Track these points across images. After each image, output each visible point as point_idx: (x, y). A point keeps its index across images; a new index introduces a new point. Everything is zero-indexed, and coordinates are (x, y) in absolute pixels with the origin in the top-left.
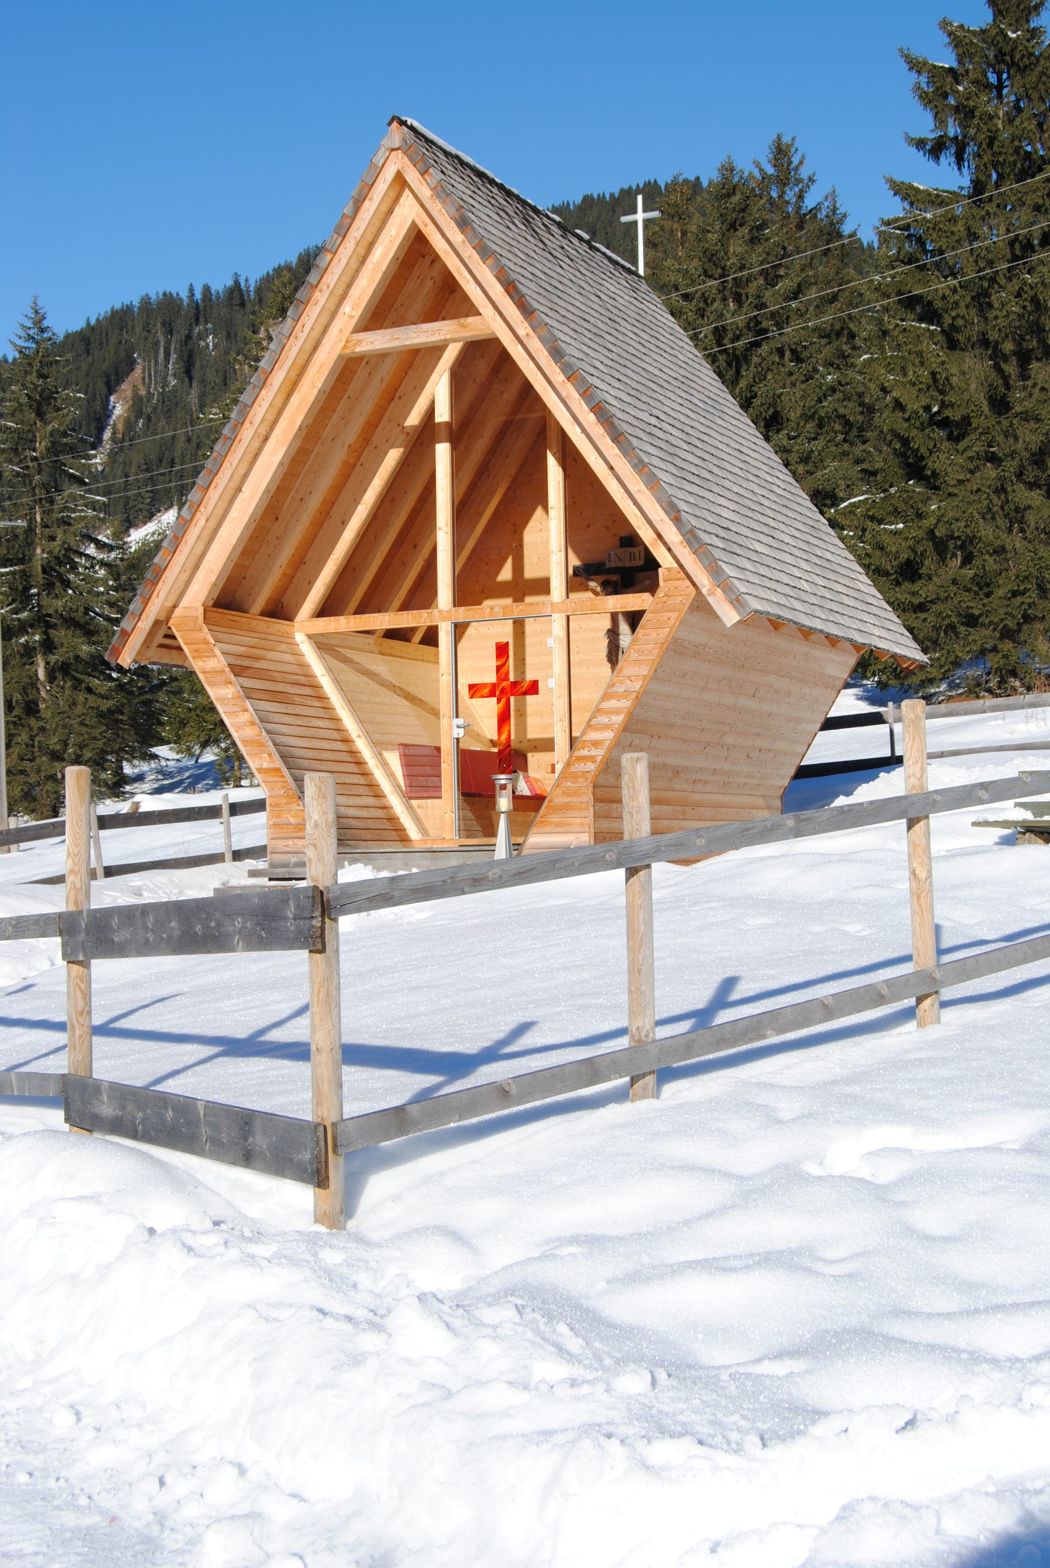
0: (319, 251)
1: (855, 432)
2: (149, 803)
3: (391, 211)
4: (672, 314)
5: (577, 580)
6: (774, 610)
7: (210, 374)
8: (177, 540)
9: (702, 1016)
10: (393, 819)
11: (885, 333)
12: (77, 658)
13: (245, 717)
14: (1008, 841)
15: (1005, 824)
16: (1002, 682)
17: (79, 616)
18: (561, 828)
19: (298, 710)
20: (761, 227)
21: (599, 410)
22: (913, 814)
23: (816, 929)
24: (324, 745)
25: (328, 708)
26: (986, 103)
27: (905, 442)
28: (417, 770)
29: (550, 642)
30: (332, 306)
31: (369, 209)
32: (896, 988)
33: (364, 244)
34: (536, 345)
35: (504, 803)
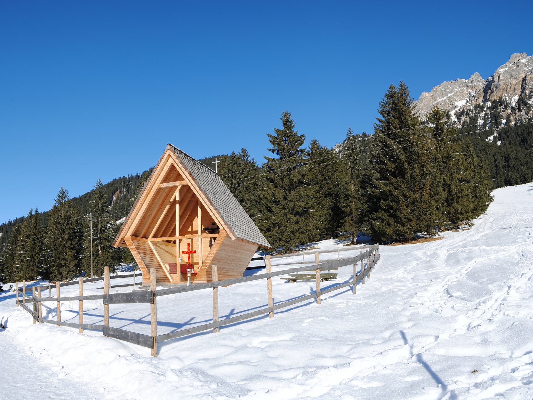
0: (153, 168)
1: (258, 203)
2: (120, 274)
3: (167, 161)
4: (222, 180)
5: (204, 231)
6: (242, 237)
7: (132, 191)
8: (126, 223)
9: (228, 316)
10: (167, 278)
11: (264, 184)
12: (106, 246)
13: (138, 257)
14: (287, 282)
15: (286, 279)
16: (286, 251)
17: (107, 238)
18: (200, 279)
19: (149, 256)
20: (240, 164)
21: (208, 198)
22: (268, 277)
23: (250, 299)
24: (154, 263)
25: (155, 256)
26: (283, 143)
27: (267, 205)
28: (172, 268)
29: (198, 243)
30: (156, 179)
31: (163, 160)
32: (265, 311)
33: (162, 167)
34: (196, 186)
35: (189, 275)
